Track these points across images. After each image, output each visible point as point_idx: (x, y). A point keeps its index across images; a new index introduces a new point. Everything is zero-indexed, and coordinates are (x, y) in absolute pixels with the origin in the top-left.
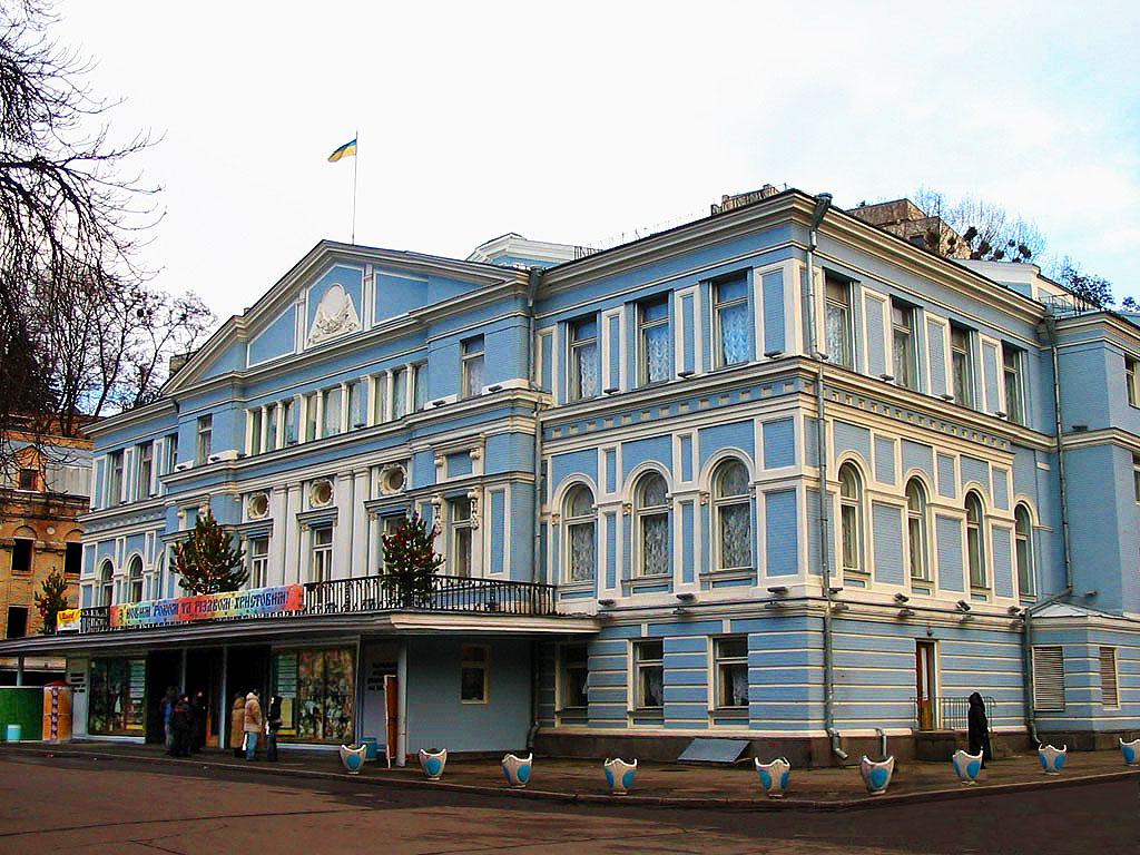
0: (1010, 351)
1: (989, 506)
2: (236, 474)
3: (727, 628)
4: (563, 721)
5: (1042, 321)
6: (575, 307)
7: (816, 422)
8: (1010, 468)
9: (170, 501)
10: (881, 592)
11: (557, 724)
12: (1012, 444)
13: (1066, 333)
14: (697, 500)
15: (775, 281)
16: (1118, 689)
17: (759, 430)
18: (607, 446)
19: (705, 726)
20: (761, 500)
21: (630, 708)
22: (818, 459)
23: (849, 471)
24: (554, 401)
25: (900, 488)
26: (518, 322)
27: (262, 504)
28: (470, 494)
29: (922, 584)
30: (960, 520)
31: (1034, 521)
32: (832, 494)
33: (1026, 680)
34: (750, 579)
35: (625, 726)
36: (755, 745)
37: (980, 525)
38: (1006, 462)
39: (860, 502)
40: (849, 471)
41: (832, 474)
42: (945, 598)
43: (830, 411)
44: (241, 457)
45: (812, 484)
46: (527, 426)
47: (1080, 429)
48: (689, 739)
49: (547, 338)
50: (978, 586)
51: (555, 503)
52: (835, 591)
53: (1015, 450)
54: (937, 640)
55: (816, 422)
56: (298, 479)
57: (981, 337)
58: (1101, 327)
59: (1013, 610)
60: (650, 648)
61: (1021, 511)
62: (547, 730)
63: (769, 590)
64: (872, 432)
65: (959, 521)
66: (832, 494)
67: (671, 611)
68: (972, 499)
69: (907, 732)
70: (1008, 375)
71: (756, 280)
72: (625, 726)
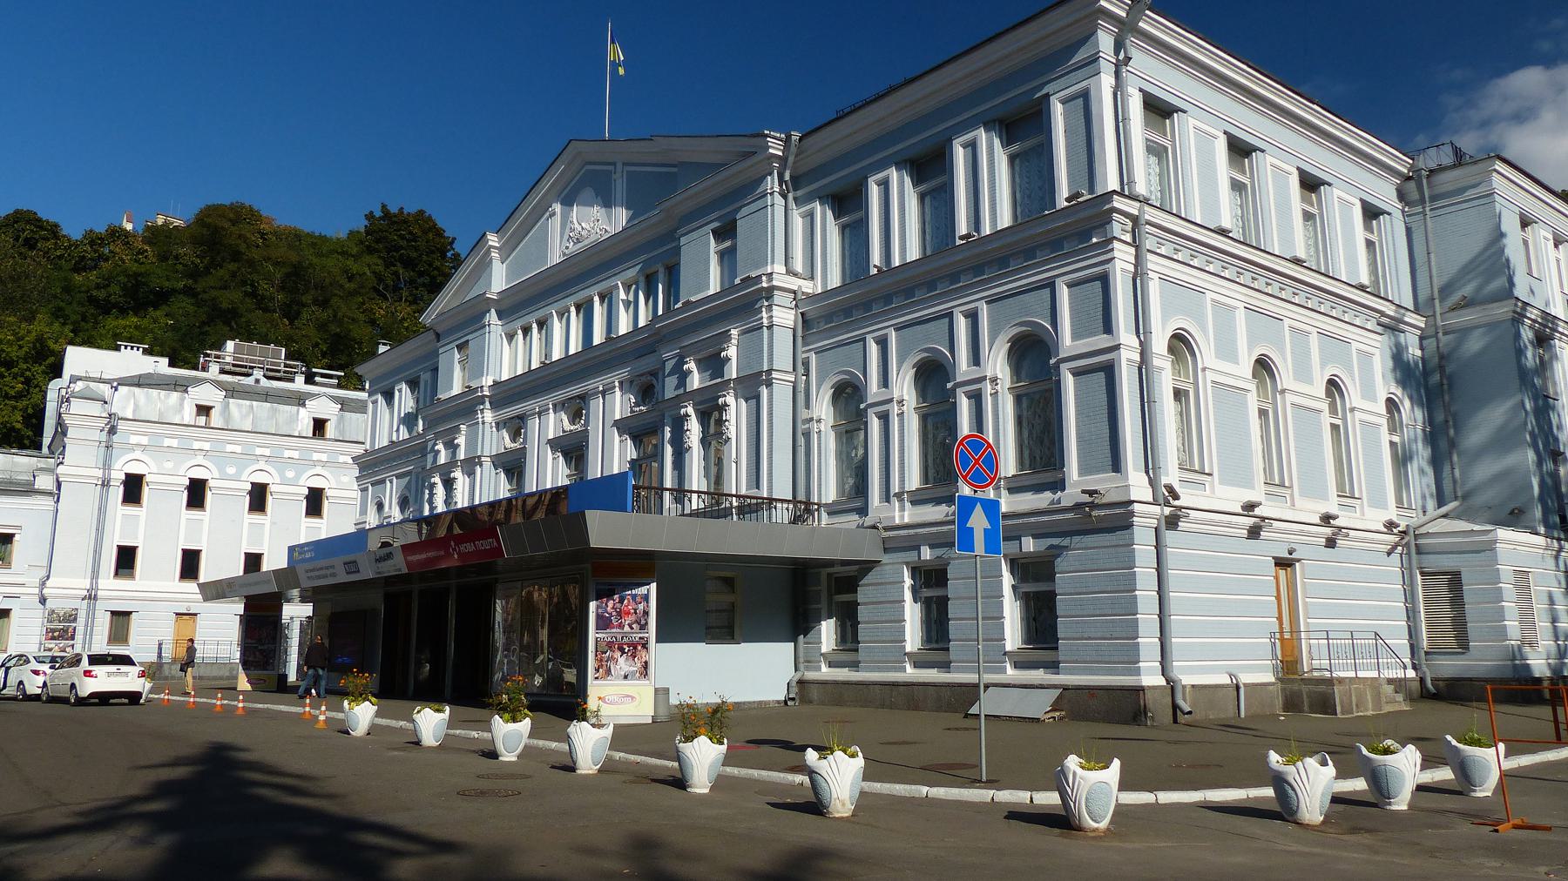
0: (1371, 213)
5: (1409, 178)
7: (1139, 274)
8: (1377, 352)
10: (1233, 498)
17: (1064, 294)
20: (1069, 382)
25: (1246, 367)
37: (1344, 419)
39: (1196, 384)
40: (1180, 344)
41: (1159, 344)
50: (1346, 492)
54: (1299, 560)
57: (1336, 192)
63: (1084, 492)
70: (1370, 244)
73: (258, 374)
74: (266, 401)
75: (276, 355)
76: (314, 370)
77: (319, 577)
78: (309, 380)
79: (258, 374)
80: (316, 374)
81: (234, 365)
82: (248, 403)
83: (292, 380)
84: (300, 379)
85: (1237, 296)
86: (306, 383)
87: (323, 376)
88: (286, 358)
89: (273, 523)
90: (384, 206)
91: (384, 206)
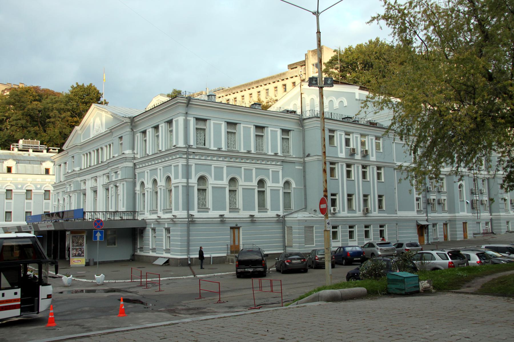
0: (285, 131)
1: (269, 184)
2: (79, 175)
3: (166, 226)
4: (140, 251)
6: (142, 128)
9: (65, 182)
11: (138, 251)
12: (282, 162)
13: (306, 124)
14: (162, 189)
15: (177, 121)
16: (314, 239)
18: (147, 171)
19: (162, 254)
21: (151, 248)
22: (187, 175)
23: (202, 179)
24: (138, 156)
26: (128, 133)
27: (85, 183)
28: (117, 185)
29: (233, 209)
30: (254, 189)
31: (294, 185)
32: (193, 187)
33: (284, 237)
34: (171, 212)
35: (149, 253)
36: (170, 260)
37: (266, 189)
38: (279, 169)
40: (202, 179)
41: (194, 180)
42: (244, 214)
43: (192, 162)
44: (81, 169)
45: (185, 184)
46: (131, 165)
47: (308, 156)
48: (158, 257)
49: (138, 137)
51: (138, 188)
52: (192, 215)
53: (284, 164)
55: (187, 167)
56: (90, 177)
58: (316, 122)
59: (278, 216)
60: (154, 230)
61: (287, 184)
62: (136, 253)
64: (213, 166)
65: (254, 189)
66: (193, 187)
67: (154, 220)
68: (261, 183)
69: (225, 255)
71: (174, 122)
72: (149, 253)
73: (31, 151)
74: (30, 163)
75: (37, 143)
76: (50, 148)
77: (25, 229)
78: (48, 151)
79: (31, 151)
80: (50, 149)
81: (23, 148)
82: (24, 165)
83: (42, 152)
84: (45, 151)
85: (224, 165)
86: (47, 152)
87: (53, 149)
88: (40, 144)
89: (34, 202)
90: (77, 83)
91: (77, 83)
